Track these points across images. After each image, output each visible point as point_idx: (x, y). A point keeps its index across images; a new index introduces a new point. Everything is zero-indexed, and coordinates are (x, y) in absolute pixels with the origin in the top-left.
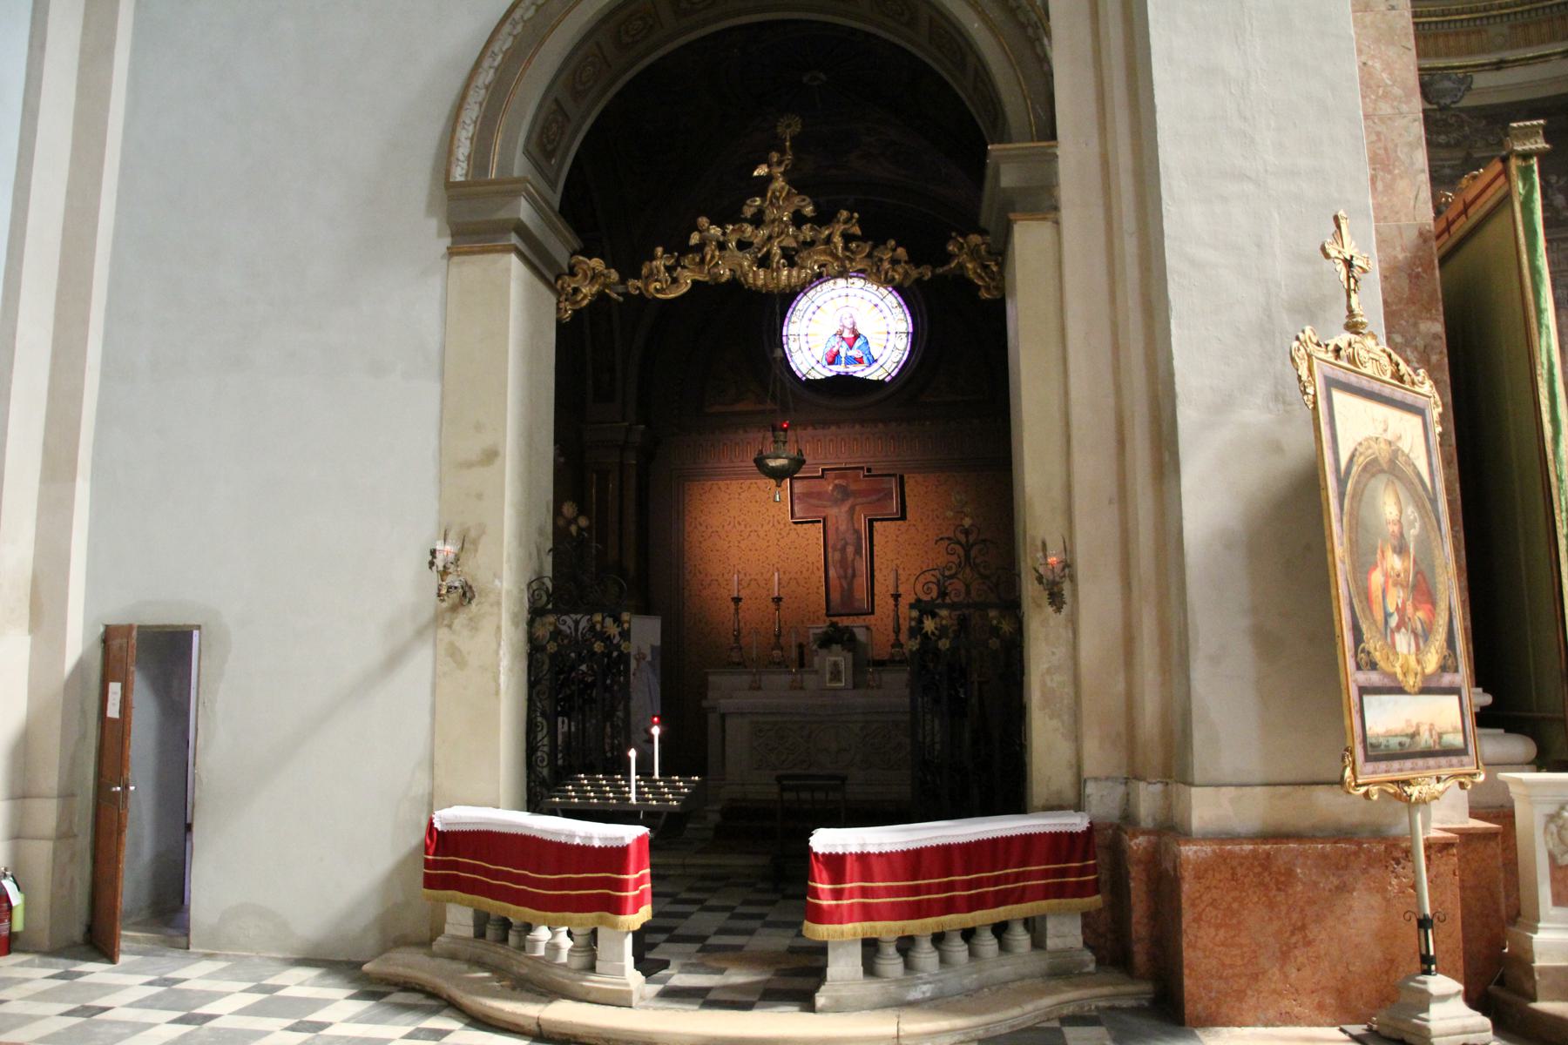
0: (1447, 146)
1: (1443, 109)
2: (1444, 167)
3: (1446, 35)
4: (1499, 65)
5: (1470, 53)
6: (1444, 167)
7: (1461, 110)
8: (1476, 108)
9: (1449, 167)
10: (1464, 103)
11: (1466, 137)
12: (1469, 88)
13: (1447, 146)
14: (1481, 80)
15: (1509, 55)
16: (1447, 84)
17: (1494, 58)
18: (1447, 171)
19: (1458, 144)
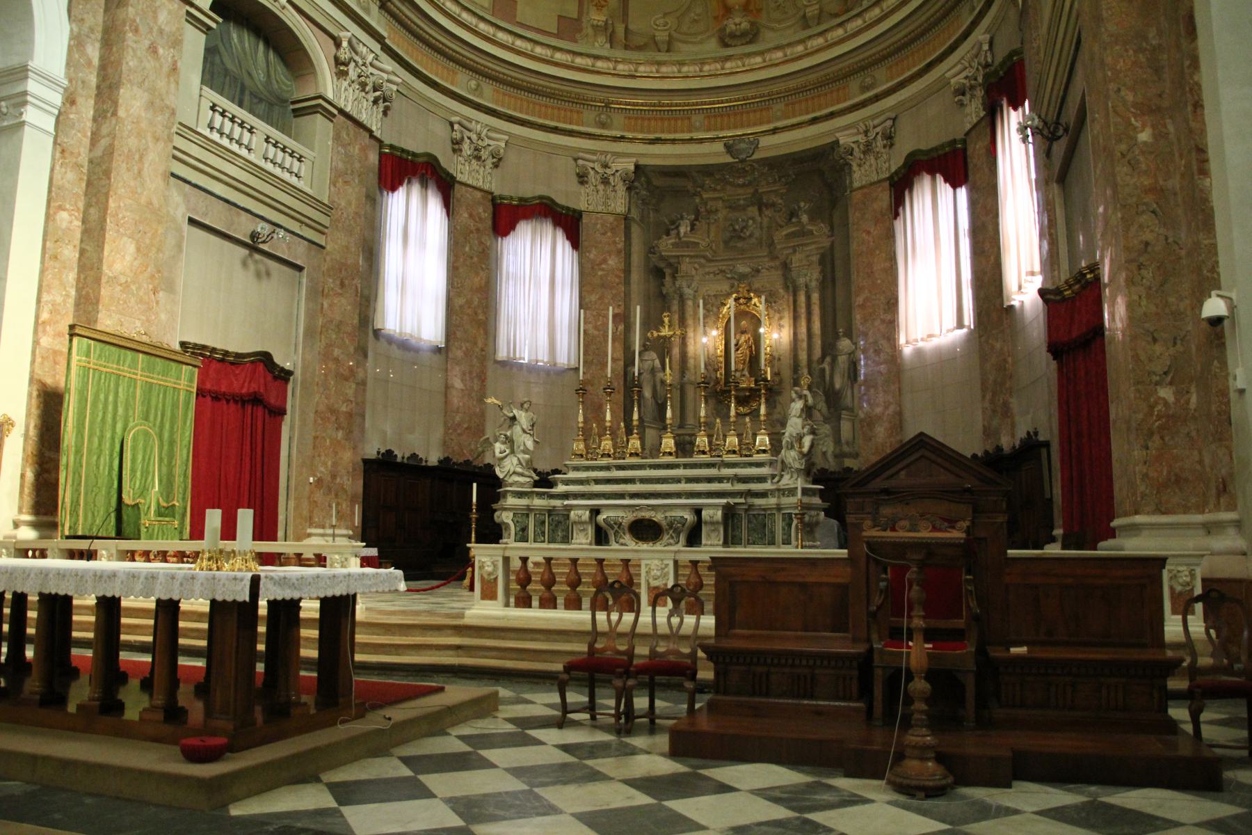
0: (743, 186)
1: (742, 161)
2: (739, 200)
3: (755, 111)
4: (775, 131)
5: (761, 124)
6: (739, 200)
7: (754, 161)
8: (761, 159)
9: (744, 199)
10: (754, 157)
11: (755, 179)
12: (757, 147)
13: (743, 186)
14: (765, 141)
15: (779, 124)
16: (743, 146)
17: (771, 126)
18: (742, 202)
19: (750, 183)
